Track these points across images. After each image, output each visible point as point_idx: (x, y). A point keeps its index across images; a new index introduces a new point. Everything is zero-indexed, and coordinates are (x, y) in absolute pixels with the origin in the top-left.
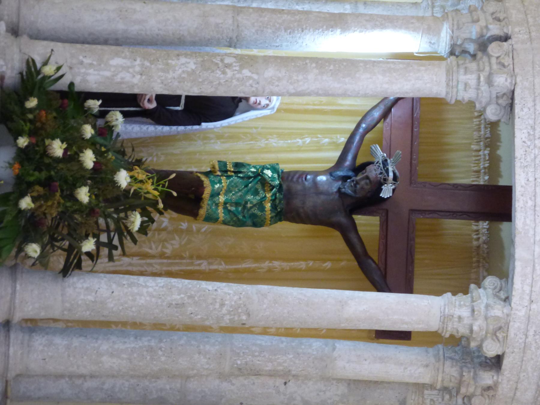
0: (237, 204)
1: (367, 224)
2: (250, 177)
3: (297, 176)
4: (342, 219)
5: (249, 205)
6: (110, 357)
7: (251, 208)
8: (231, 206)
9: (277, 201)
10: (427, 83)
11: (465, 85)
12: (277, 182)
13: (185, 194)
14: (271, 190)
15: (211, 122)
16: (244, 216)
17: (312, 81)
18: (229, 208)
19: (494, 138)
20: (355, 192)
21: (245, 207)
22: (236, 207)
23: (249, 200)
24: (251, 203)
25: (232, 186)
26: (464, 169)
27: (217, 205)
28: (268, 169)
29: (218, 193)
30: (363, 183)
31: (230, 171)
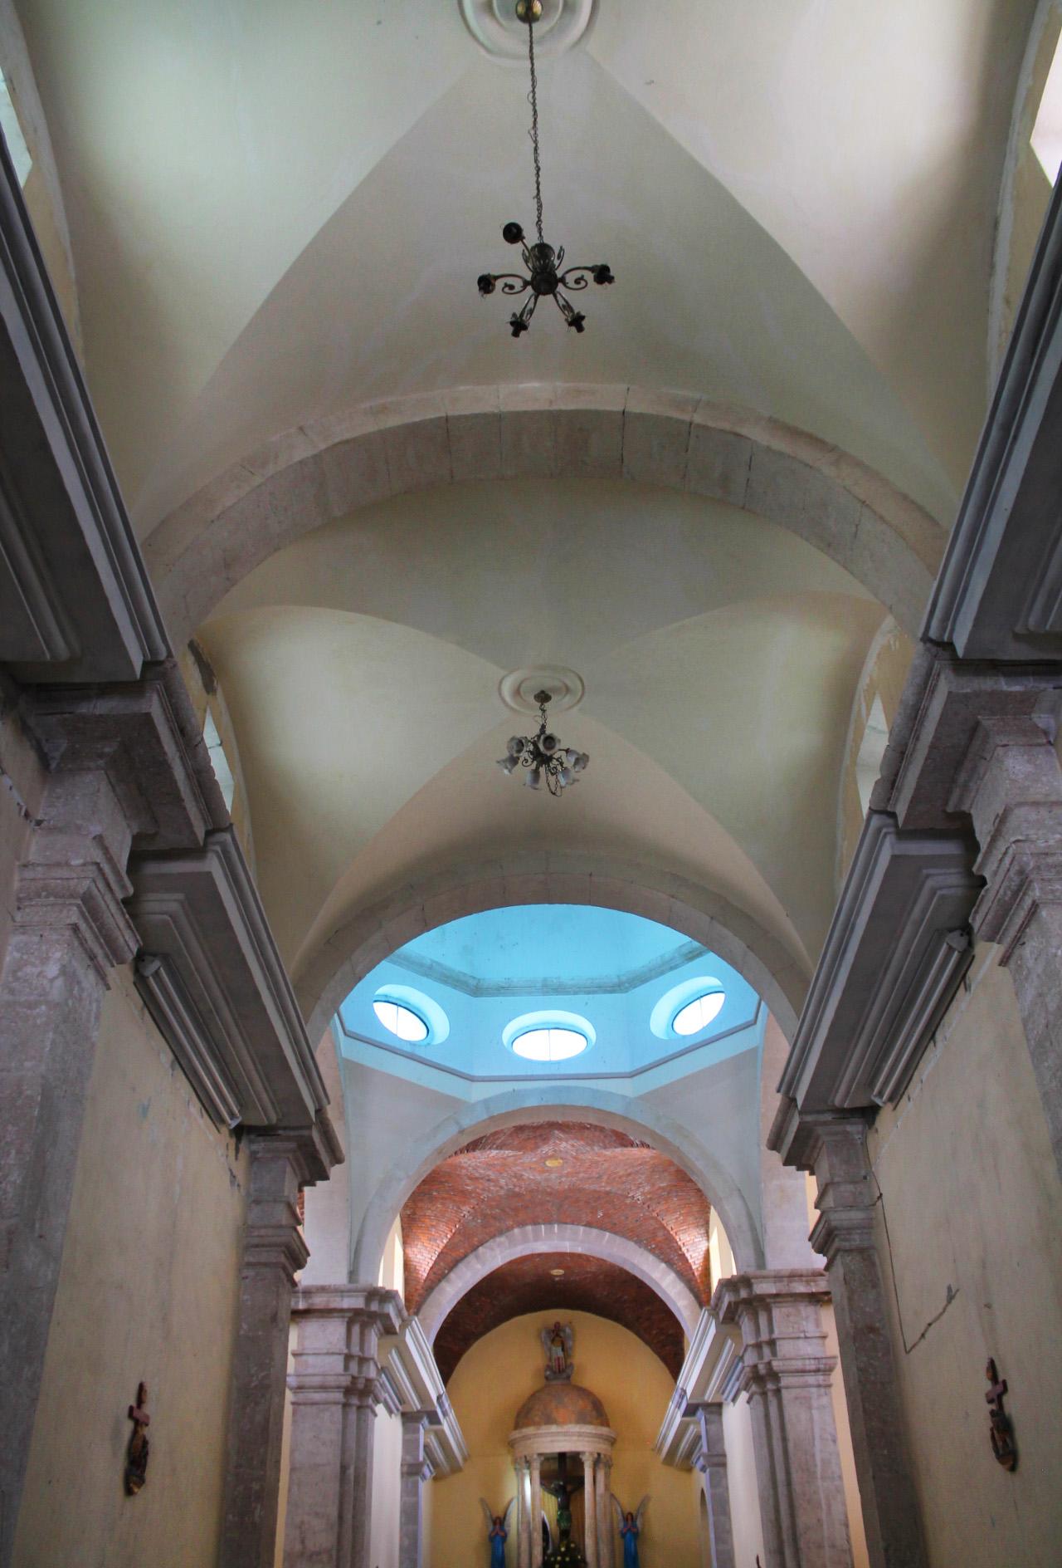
1: (569, 1488)
6: (604, 1551)
10: (536, 1474)
11: (536, 1465)
13: (565, 1534)
17: (538, 1503)
19: (547, 1458)
26: (555, 1466)
29: (564, 1525)
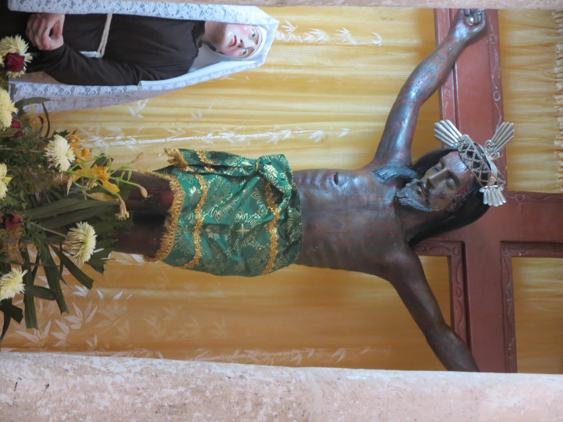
0: (222, 228)
2: (241, 178)
3: (319, 177)
4: (399, 256)
5: (243, 230)
7: (246, 235)
8: (214, 231)
9: (290, 224)
12: (289, 187)
14: (279, 202)
15: (162, 78)
16: (234, 252)
18: (210, 235)
20: (427, 203)
21: (234, 234)
22: (220, 234)
23: (242, 221)
24: (247, 225)
25: (215, 193)
27: (191, 228)
28: (269, 164)
30: (442, 185)
31: (207, 165)
